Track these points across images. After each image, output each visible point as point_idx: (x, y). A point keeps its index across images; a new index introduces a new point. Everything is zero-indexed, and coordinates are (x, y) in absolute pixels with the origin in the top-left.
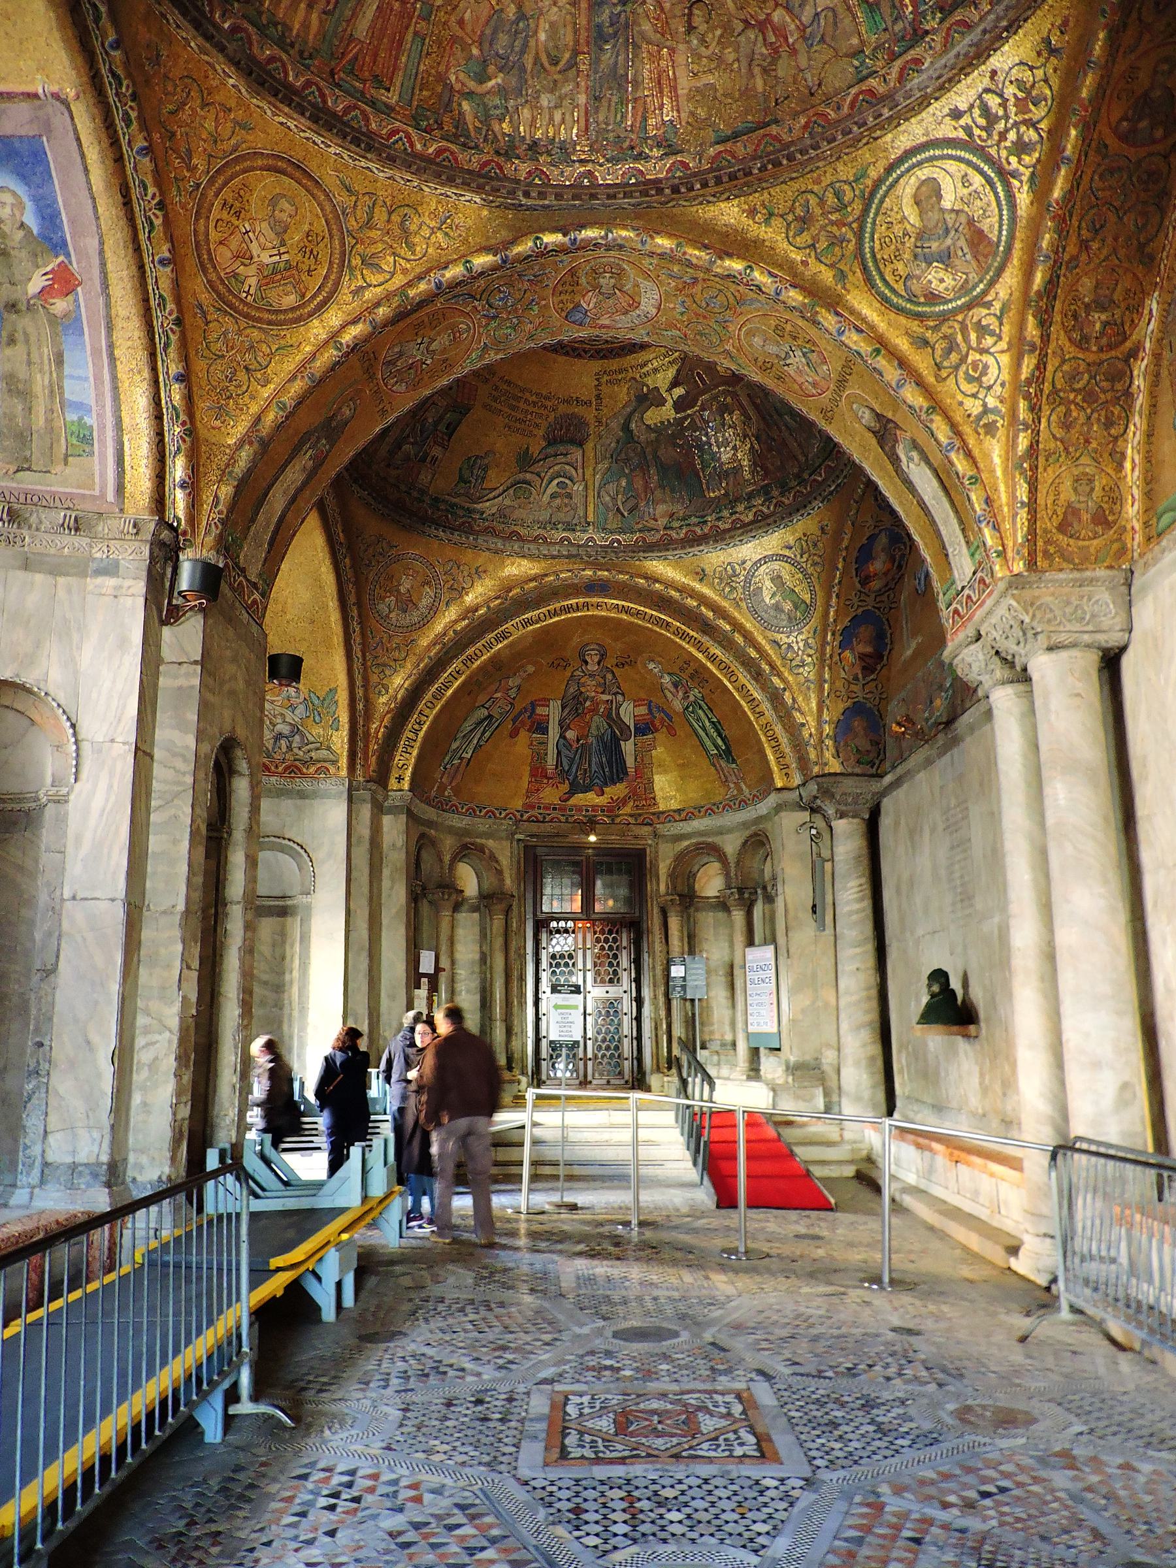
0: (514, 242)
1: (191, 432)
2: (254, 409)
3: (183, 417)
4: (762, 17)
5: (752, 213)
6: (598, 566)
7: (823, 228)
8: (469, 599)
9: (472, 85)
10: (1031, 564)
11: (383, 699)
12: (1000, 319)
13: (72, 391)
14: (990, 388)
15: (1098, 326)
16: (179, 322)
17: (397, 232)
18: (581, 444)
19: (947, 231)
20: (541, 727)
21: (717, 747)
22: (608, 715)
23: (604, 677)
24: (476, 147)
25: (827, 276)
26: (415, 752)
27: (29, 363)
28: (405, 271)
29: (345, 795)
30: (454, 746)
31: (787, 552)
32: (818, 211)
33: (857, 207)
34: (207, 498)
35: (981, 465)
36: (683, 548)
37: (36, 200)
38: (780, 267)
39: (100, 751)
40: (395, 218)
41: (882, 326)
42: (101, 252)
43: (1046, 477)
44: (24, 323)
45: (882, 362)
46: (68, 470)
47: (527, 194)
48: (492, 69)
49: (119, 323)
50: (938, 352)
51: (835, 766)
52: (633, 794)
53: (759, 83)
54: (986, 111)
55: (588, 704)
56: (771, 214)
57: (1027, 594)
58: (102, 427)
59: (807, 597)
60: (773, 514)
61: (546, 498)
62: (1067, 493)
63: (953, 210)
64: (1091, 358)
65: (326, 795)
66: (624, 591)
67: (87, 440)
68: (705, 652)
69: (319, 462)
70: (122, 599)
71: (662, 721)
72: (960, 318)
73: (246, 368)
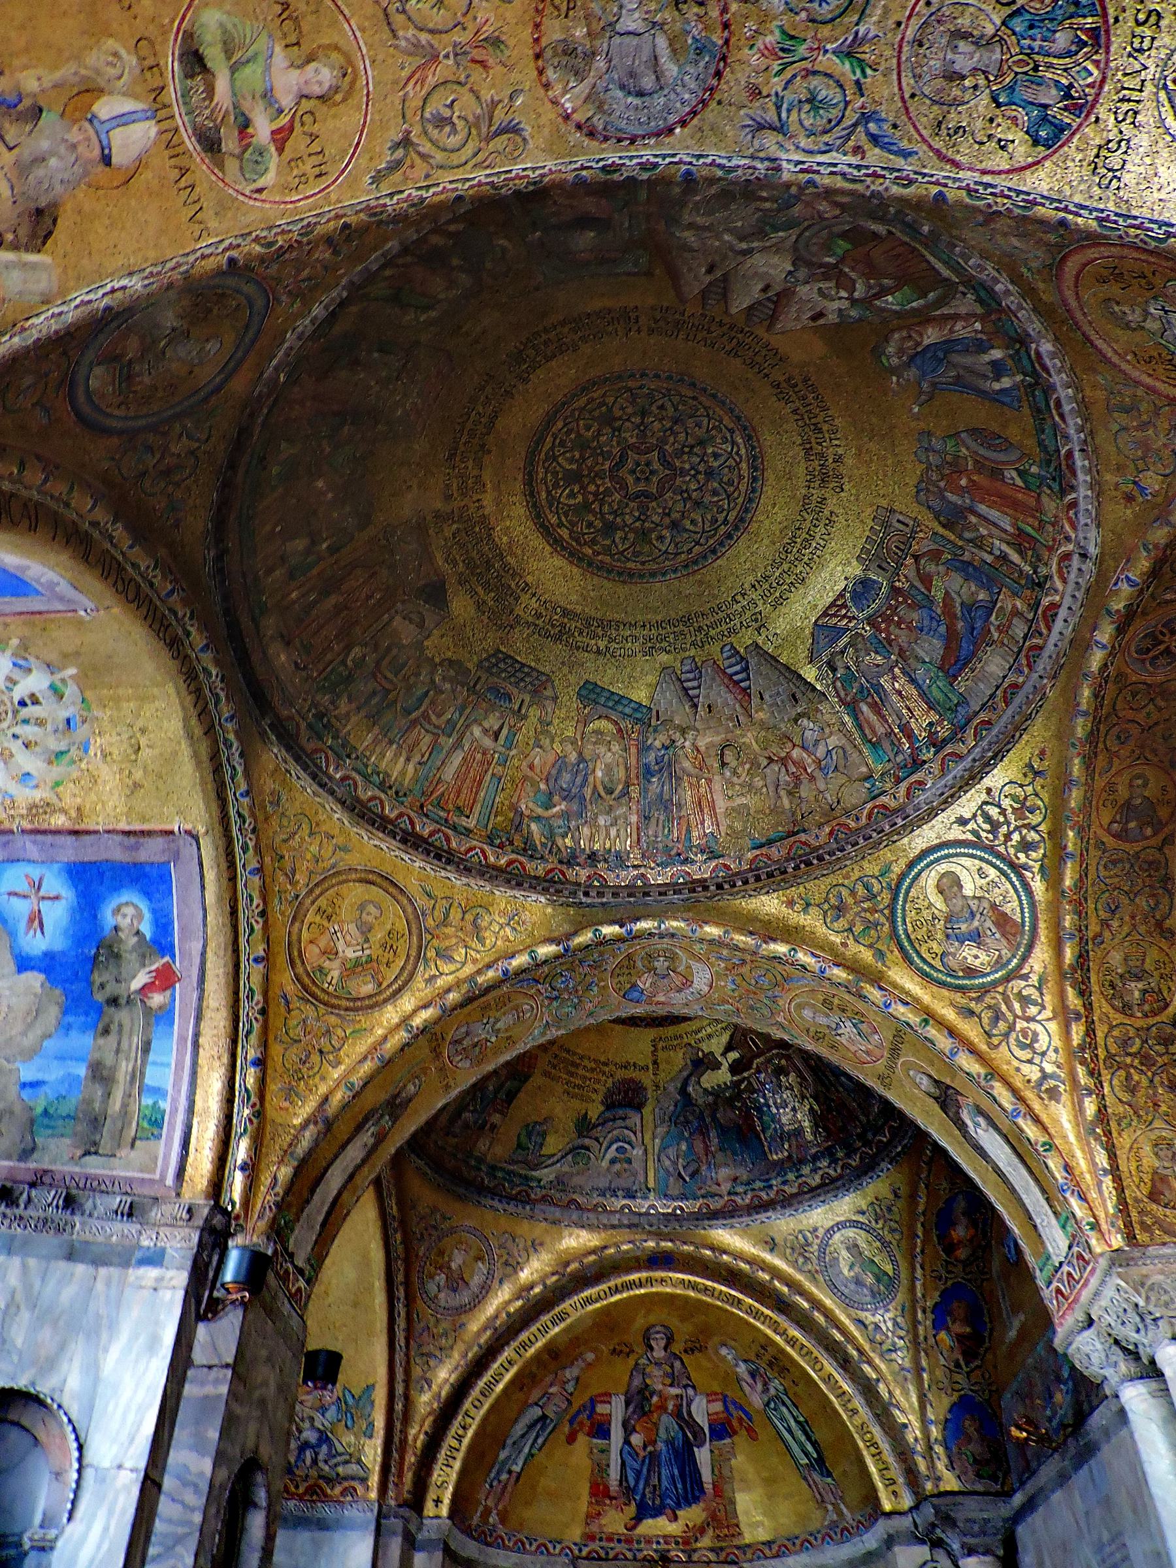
0: (575, 933)
1: (259, 1114)
2: (323, 1089)
3: (253, 1099)
4: (783, 755)
5: (790, 903)
6: (660, 1236)
7: (857, 914)
8: (525, 1275)
9: (540, 811)
10: (1130, 1237)
11: (425, 1398)
12: (1039, 989)
13: (152, 1077)
14: (1043, 1054)
15: (1137, 994)
16: (263, 1012)
17: (469, 927)
18: (639, 1107)
19: (973, 915)
20: (601, 1430)
21: (807, 1454)
22: (678, 1414)
23: (672, 1367)
24: (542, 858)
25: (867, 956)
26: (457, 1465)
27: (118, 1051)
28: (475, 961)
29: (372, 1527)
30: (503, 1455)
31: (861, 1218)
32: (850, 901)
33: (886, 897)
34: (266, 1180)
35: (1052, 1131)
36: (749, 1215)
37: (154, 911)
38: (822, 949)
39: (103, 1480)
40: (469, 917)
41: (926, 998)
42: (203, 954)
43: (1123, 1141)
44: (122, 1016)
45: (932, 1032)
46: (133, 1154)
47: (586, 894)
48: (556, 798)
49: (208, 1014)
50: (985, 1021)
51: (950, 1482)
52: (713, 1520)
53: (786, 802)
54: (988, 818)
55: (655, 1399)
56: (808, 905)
57: (1135, 1272)
58: (174, 1110)
59: (889, 1268)
60: (840, 1177)
61: (605, 1164)
62: (1149, 1160)
63: (974, 897)
64: (1140, 1023)
65: (351, 1526)
67: (157, 1123)
68: (783, 1333)
69: (380, 1138)
70: (161, 1293)
71: (740, 1420)
72: (1000, 989)
73: (321, 1052)
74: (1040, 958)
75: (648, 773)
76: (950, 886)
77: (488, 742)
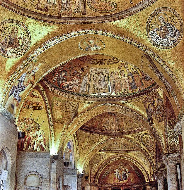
66: (125, 156)
74: (154, 146)
75: (116, 121)
76: (146, 137)
77: (98, 120)
